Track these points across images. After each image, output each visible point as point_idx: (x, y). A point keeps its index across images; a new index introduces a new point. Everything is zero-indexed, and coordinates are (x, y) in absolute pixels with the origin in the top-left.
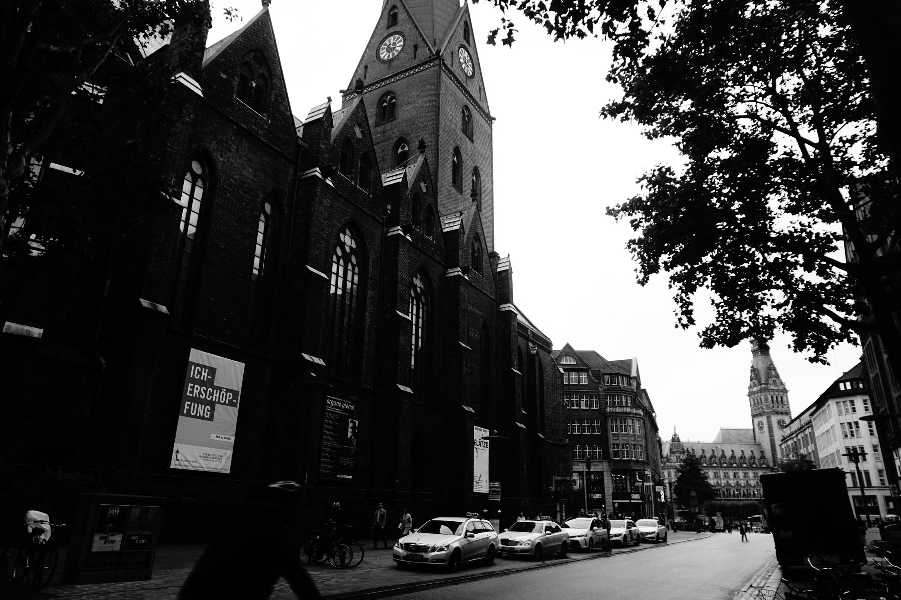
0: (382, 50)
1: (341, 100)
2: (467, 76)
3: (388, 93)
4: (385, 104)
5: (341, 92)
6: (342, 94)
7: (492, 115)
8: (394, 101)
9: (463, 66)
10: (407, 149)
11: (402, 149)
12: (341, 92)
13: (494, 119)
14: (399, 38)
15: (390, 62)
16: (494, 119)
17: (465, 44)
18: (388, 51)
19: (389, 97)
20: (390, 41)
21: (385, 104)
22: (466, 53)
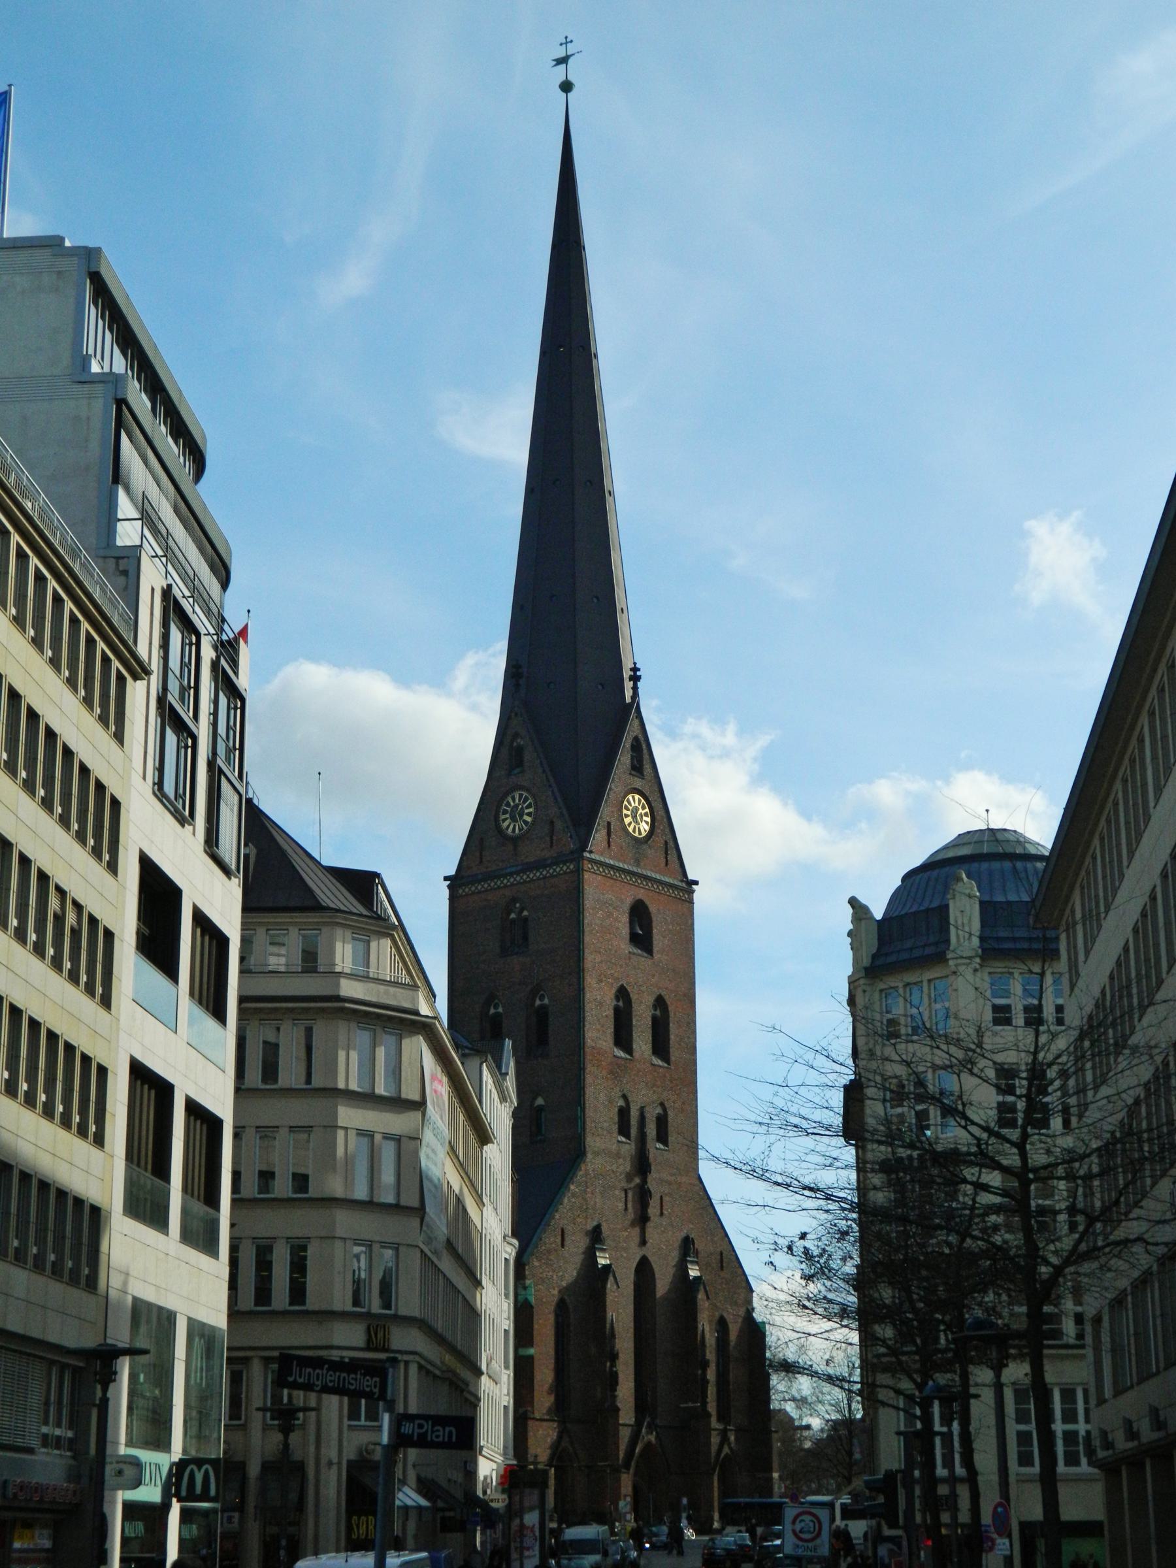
0: (503, 814)
1: (446, 892)
2: (636, 839)
3: (514, 900)
4: (513, 916)
5: (446, 879)
6: (448, 882)
7: (691, 876)
8: (525, 913)
9: (630, 829)
10: (546, 1001)
11: (540, 1000)
12: (446, 879)
13: (696, 883)
14: (526, 799)
15: (515, 840)
16: (696, 883)
17: (638, 783)
18: (513, 819)
19: (518, 905)
20: (514, 799)
21: (513, 916)
22: (637, 797)
